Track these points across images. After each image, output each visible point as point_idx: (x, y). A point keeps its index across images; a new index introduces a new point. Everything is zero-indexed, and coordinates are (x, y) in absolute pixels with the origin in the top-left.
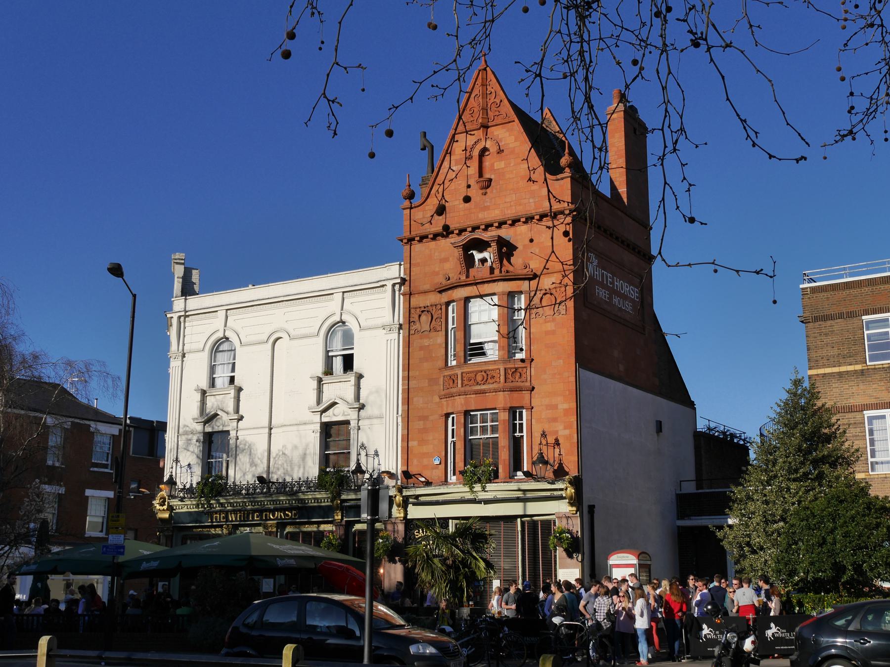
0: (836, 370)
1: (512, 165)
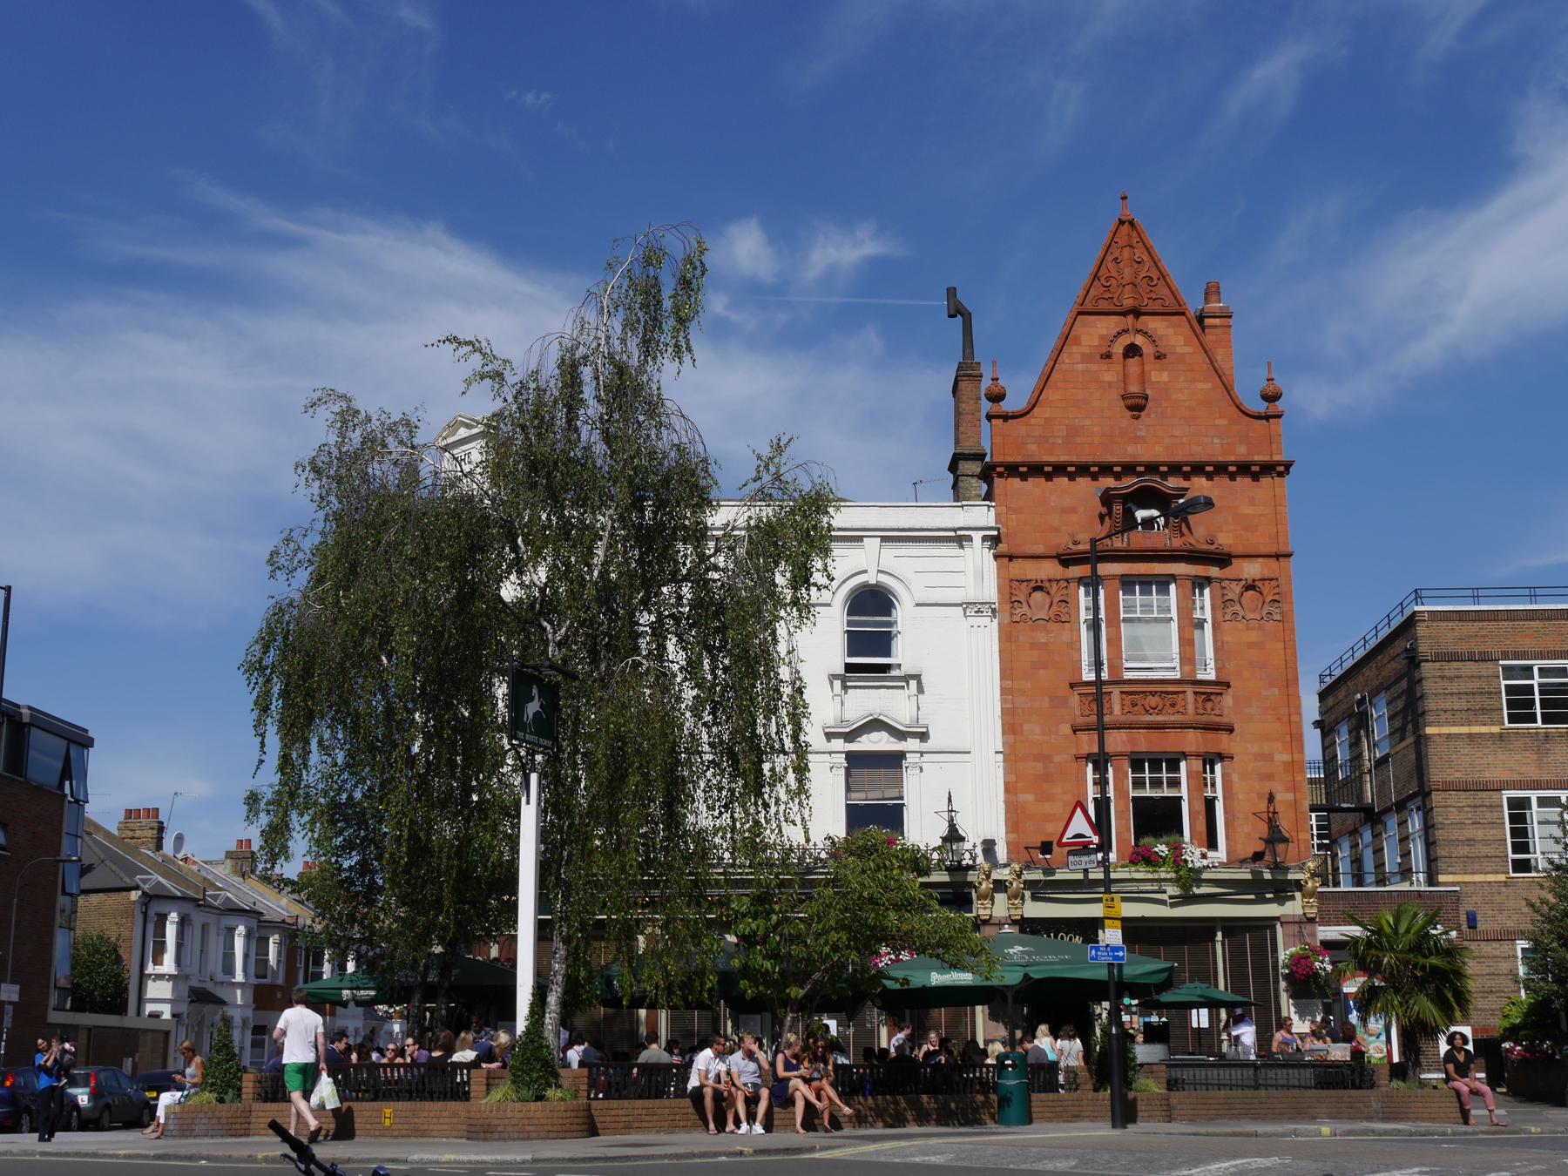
0: (1465, 730)
1: (1181, 380)
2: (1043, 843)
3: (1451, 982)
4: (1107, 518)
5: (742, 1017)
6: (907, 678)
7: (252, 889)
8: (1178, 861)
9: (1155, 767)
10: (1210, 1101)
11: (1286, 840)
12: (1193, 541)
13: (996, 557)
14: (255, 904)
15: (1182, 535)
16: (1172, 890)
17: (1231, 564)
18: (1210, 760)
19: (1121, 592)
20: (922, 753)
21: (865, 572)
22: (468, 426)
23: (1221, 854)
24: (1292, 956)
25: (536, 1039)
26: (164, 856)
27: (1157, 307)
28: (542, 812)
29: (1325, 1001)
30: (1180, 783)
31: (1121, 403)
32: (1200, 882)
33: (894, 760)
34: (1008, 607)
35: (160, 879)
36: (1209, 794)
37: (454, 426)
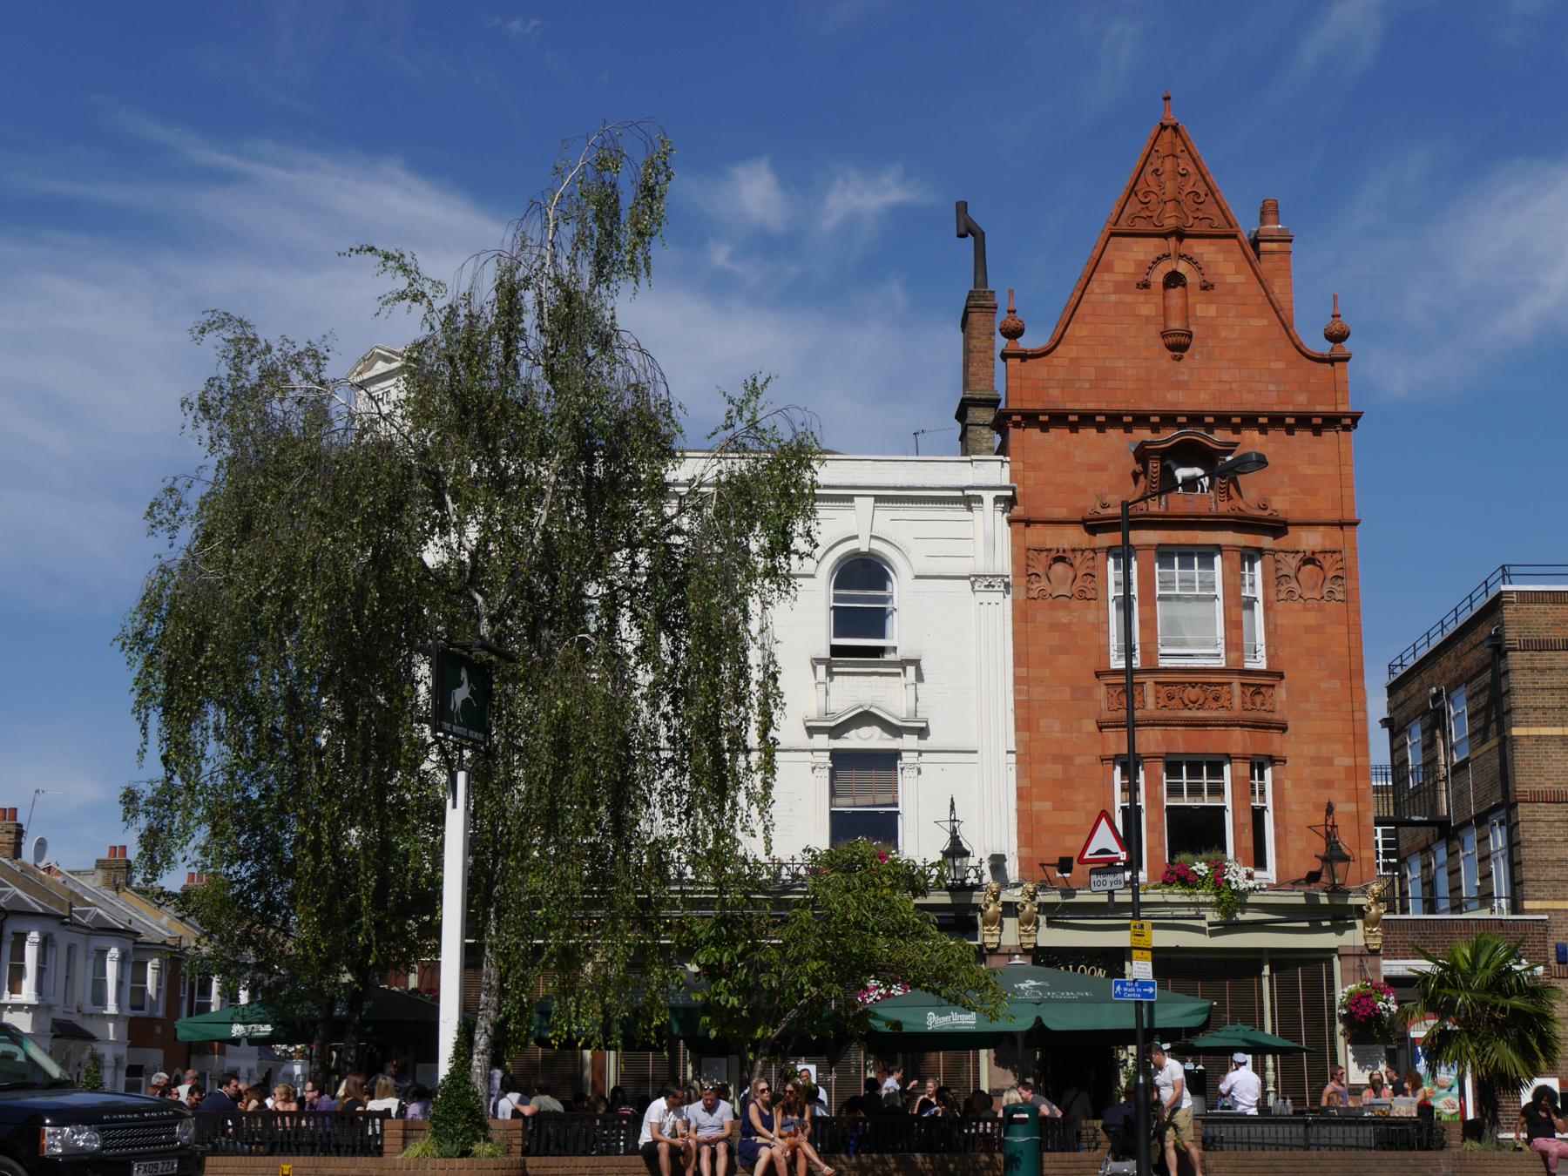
0: (1557, 731)
2: (1061, 859)
3: (1534, 1028)
4: (1142, 478)
5: (704, 1061)
6: (903, 664)
7: (127, 904)
8: (1218, 881)
9: (1195, 771)
10: (1253, 1163)
11: (1346, 859)
12: (1242, 506)
13: (1010, 521)
14: (130, 922)
15: (1230, 498)
16: (1212, 916)
17: (1287, 533)
18: (1259, 763)
19: (1157, 565)
20: (920, 752)
21: (856, 537)
22: (387, 360)
23: (1270, 874)
24: (1350, 994)
25: (462, 1084)
26: (23, 864)
27: (1204, 228)
28: (473, 816)
29: (1389, 1046)
30: (1223, 790)
31: (1161, 342)
32: (1245, 907)
33: (887, 761)
34: (1024, 580)
35: (19, 892)
36: (1257, 804)
37: (370, 359)
